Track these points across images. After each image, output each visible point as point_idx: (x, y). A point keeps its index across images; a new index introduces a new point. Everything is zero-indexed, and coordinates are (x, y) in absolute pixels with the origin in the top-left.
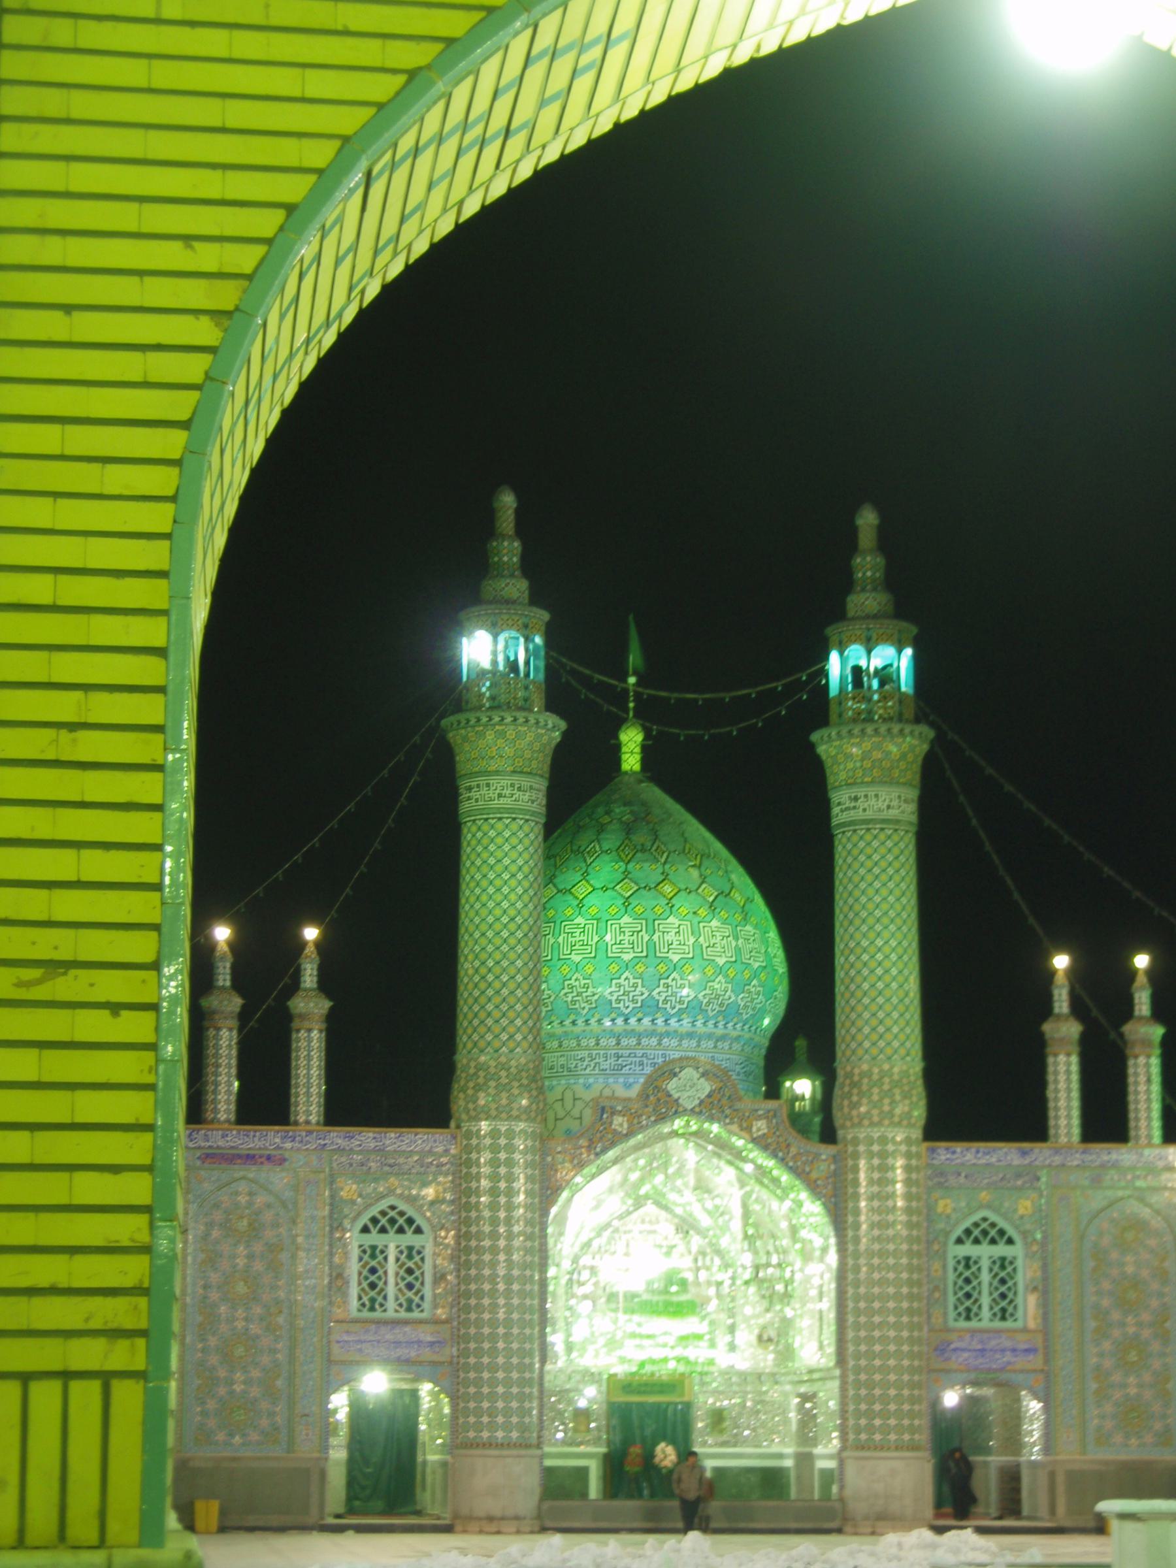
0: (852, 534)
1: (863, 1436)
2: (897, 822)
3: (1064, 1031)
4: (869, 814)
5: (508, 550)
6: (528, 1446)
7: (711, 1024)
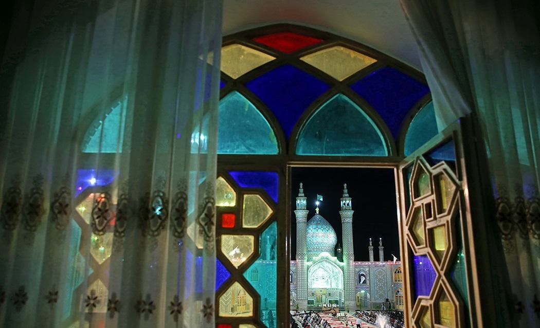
0: (343, 187)
3: (371, 248)
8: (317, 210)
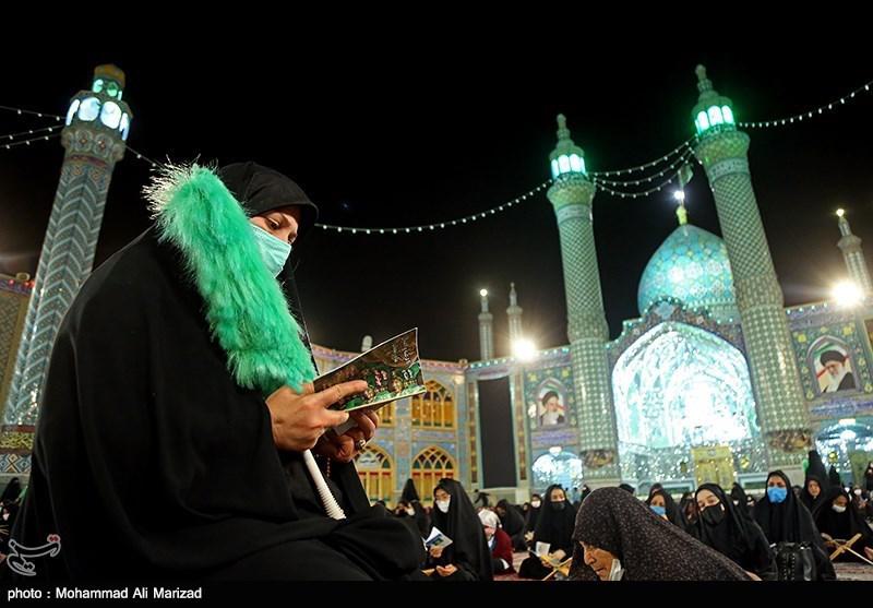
1: (776, 459)
2: (734, 174)
4: (722, 174)
5: (563, 132)
6: (615, 477)
7: (719, 300)
8: (681, 213)
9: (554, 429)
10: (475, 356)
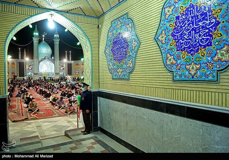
8: (43, 39)
9: (30, 70)
10: (18, 58)
